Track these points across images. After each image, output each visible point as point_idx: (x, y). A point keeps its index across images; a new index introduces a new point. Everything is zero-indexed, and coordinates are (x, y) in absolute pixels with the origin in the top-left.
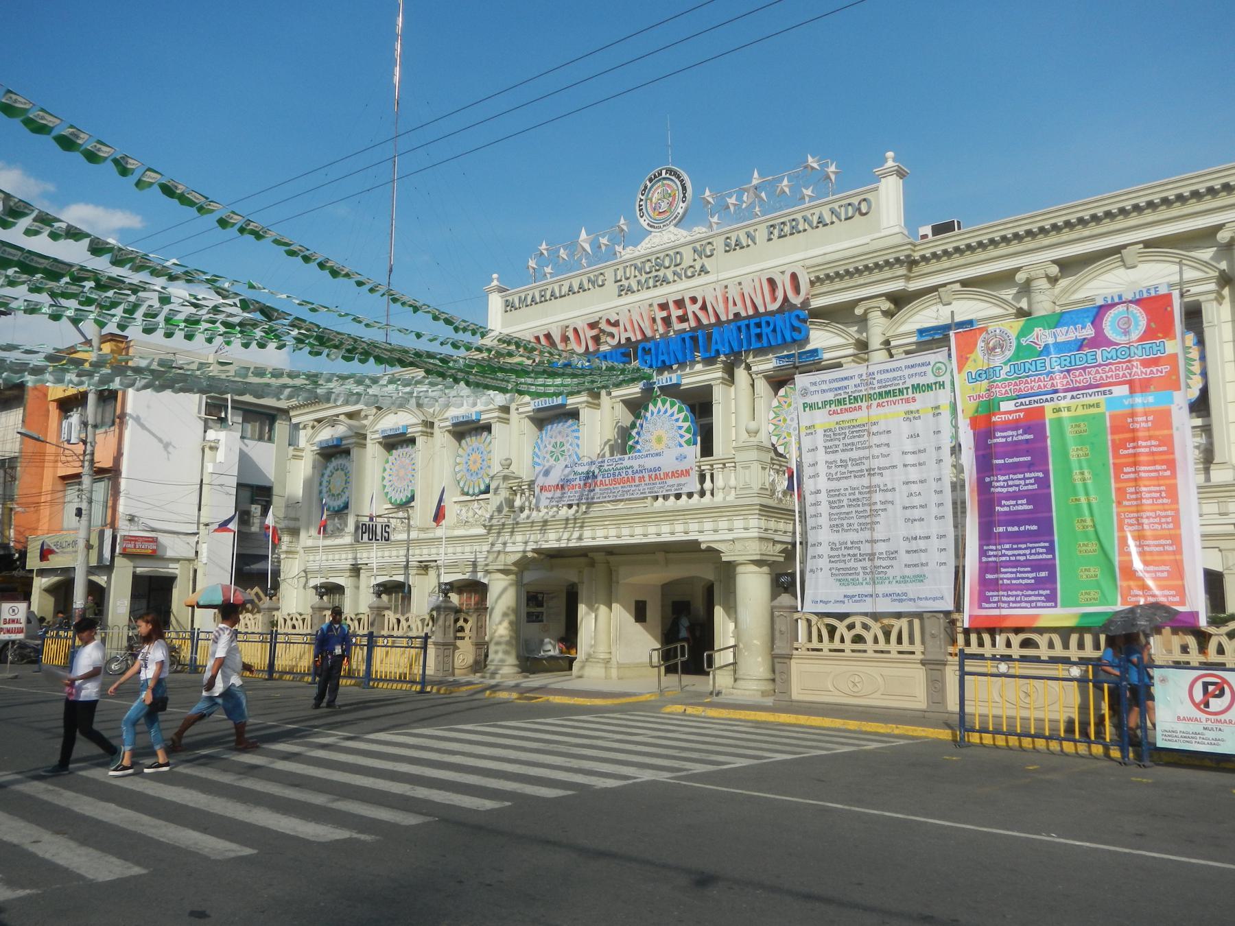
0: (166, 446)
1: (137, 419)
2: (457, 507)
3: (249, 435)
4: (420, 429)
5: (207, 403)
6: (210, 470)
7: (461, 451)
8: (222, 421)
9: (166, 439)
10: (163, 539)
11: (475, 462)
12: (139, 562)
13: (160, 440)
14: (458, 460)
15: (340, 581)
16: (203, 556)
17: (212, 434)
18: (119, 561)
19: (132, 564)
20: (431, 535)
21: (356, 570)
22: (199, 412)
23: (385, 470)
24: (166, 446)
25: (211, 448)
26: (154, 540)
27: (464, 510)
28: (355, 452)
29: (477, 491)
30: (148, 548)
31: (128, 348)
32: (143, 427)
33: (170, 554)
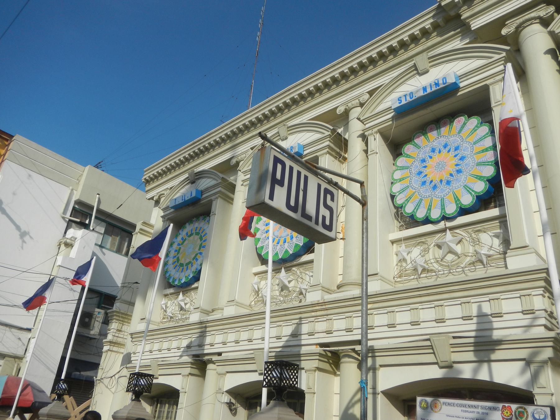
0: (23, 235)
2: (403, 248)
3: (108, 246)
4: (327, 143)
5: (74, 208)
6: (59, 263)
7: (401, 161)
8: (84, 226)
9: (24, 228)
11: (440, 166)
13: (18, 228)
14: (398, 175)
15: (175, 382)
16: (29, 355)
17: (72, 232)
21: (201, 364)
24: (23, 235)
25: (67, 245)
27: (416, 252)
28: (218, 206)
29: (451, 209)
31: (9, 144)
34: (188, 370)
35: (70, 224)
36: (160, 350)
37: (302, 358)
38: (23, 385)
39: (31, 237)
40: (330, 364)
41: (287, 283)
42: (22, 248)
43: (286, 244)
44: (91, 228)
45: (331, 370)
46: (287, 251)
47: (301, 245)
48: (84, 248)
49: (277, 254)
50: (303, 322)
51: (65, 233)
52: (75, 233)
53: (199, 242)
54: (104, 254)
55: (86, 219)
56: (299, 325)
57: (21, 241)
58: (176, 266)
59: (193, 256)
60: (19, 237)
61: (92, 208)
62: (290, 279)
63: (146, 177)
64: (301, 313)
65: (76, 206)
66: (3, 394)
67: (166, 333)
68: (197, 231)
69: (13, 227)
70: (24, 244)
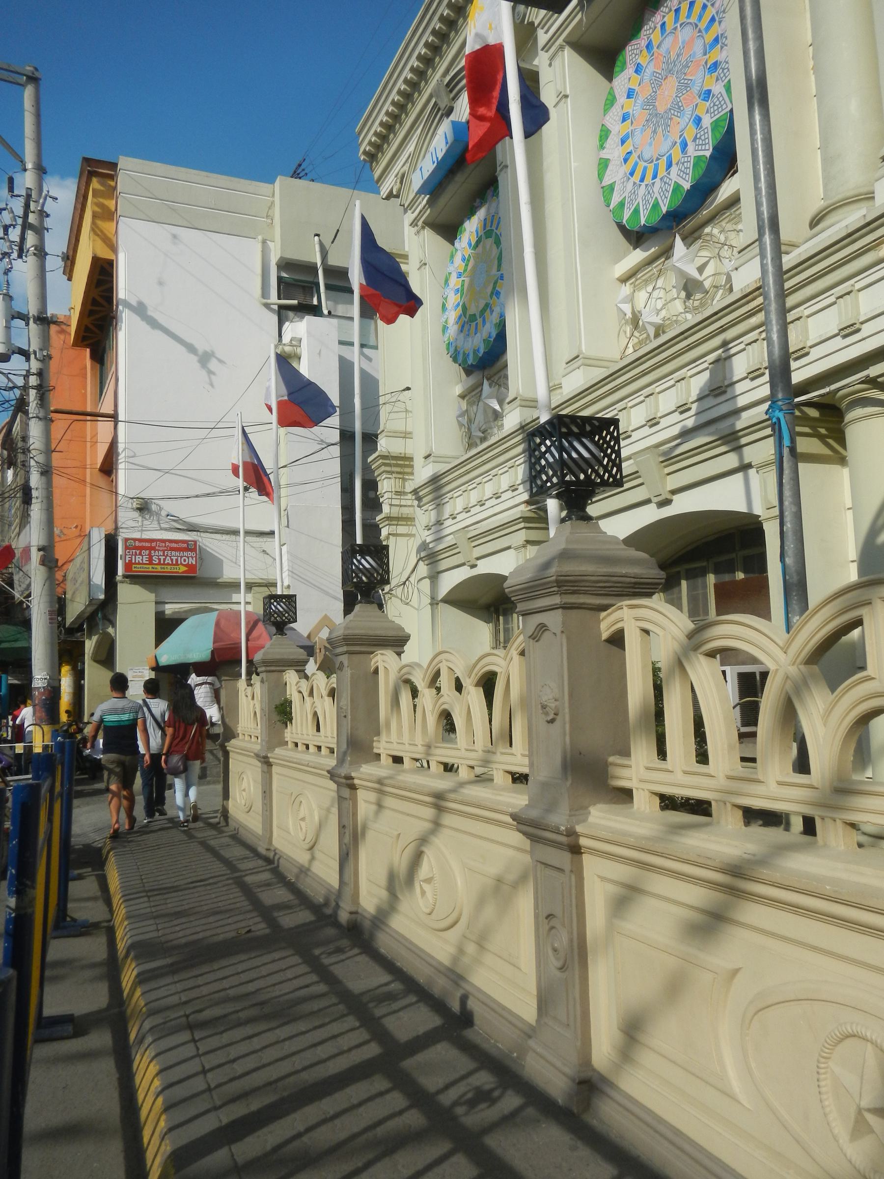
0: (205, 359)
1: (140, 310)
5: (280, 280)
9: (201, 347)
10: (208, 542)
12: (167, 593)
13: (191, 349)
18: (126, 592)
19: (152, 597)
20: (853, 217)
22: (265, 294)
23: (605, 134)
24: (205, 359)
26: (190, 547)
30: (179, 564)
32: (154, 324)
33: (229, 573)
34: (521, 536)
35: (283, 313)
36: (467, 510)
37: (744, 441)
38: (247, 623)
39: (220, 361)
40: (822, 438)
41: (695, 274)
42: (212, 385)
43: (674, 169)
44: (326, 312)
45: (826, 451)
46: (678, 186)
47: (708, 154)
48: (319, 354)
49: (656, 206)
50: (733, 351)
51: (280, 335)
52: (300, 328)
53: (495, 252)
54: (370, 360)
55: (312, 297)
56: (722, 363)
57: (204, 373)
58: (463, 327)
59: (489, 289)
60: (198, 365)
61: (313, 269)
62: (700, 261)
63: (365, 146)
64: (723, 330)
65: (284, 275)
66: (214, 643)
67: (468, 472)
68: (488, 228)
69: (183, 349)
70: (213, 377)
